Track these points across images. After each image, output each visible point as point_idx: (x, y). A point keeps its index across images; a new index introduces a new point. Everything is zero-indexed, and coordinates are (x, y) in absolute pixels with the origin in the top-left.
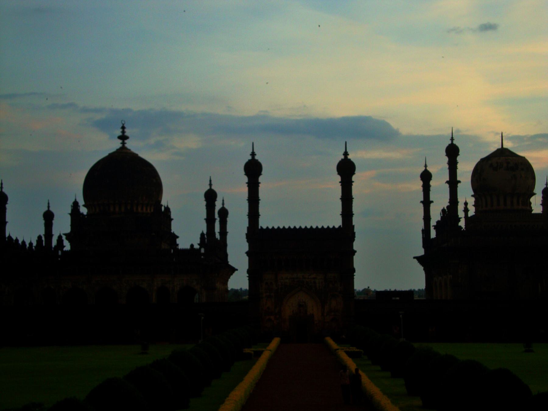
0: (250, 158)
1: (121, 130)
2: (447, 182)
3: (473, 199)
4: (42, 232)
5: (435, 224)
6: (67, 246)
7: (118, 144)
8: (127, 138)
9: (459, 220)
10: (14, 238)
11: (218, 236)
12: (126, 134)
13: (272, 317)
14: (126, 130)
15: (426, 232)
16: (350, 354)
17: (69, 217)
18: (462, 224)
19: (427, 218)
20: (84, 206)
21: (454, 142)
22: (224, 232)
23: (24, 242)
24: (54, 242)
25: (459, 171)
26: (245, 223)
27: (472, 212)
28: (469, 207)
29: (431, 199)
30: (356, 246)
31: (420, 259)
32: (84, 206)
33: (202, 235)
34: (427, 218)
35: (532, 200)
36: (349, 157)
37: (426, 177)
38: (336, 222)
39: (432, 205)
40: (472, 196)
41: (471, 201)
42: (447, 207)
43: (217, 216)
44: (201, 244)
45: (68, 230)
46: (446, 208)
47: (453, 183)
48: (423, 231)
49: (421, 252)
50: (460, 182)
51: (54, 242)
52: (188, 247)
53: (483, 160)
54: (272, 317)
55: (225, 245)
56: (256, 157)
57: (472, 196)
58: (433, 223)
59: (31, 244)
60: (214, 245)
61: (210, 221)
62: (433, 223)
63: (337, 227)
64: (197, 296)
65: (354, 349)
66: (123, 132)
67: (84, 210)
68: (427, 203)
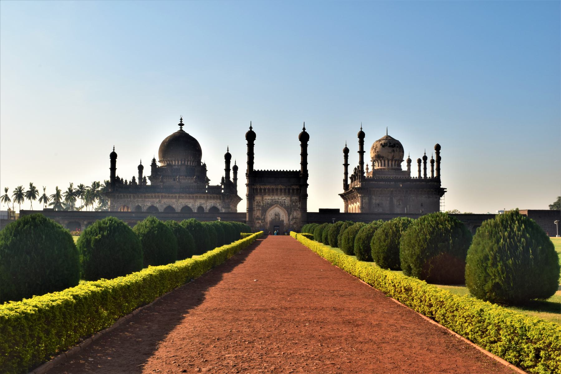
0: (249, 130)
2: (358, 152)
6: (149, 183)
7: (178, 129)
8: (183, 125)
9: (364, 173)
11: (231, 179)
13: (260, 221)
15: (346, 181)
17: (150, 167)
18: (365, 175)
20: (159, 161)
23: (126, 181)
27: (371, 169)
31: (341, 195)
32: (159, 161)
33: (223, 178)
34: (346, 173)
35: (402, 164)
37: (346, 151)
41: (370, 164)
42: (358, 167)
43: (231, 167)
44: (223, 183)
45: (150, 174)
47: (362, 152)
49: (342, 191)
53: (377, 141)
56: (253, 130)
58: (349, 175)
60: (229, 185)
61: (227, 170)
66: (181, 122)
67: (159, 164)
68: (346, 165)
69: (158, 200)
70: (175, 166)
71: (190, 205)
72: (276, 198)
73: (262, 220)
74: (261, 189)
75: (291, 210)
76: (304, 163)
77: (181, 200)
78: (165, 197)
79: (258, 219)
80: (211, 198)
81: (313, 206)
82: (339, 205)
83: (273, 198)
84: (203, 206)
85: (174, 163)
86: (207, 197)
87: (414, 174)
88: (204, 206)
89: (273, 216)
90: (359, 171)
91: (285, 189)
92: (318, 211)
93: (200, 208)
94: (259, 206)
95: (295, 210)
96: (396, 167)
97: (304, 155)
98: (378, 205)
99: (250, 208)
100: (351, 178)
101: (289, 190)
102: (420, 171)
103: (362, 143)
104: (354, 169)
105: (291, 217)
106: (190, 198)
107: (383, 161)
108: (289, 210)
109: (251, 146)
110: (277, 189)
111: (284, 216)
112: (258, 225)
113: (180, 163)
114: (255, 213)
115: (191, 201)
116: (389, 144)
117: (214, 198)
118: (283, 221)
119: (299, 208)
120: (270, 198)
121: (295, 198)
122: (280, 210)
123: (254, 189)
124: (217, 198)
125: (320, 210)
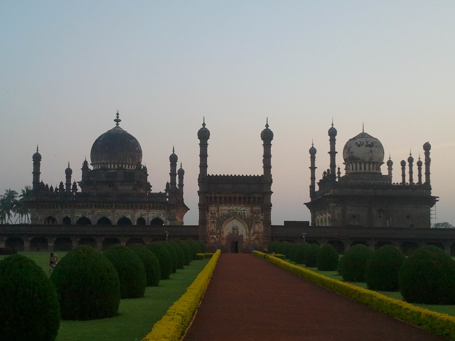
1: (116, 116)
2: (329, 153)
3: (344, 166)
5: (319, 182)
6: (79, 190)
7: (114, 125)
10: (45, 184)
12: (119, 118)
13: (215, 236)
14: (119, 116)
15: (312, 187)
18: (337, 180)
20: (91, 164)
21: (334, 127)
24: (71, 188)
25: (336, 146)
26: (197, 171)
28: (340, 170)
30: (273, 188)
32: (91, 164)
33: (168, 184)
36: (269, 128)
37: (313, 152)
38: (260, 172)
39: (316, 169)
40: (344, 163)
42: (328, 170)
46: (326, 171)
47: (333, 153)
48: (310, 186)
49: (309, 200)
50: (337, 153)
52: (158, 192)
54: (215, 236)
56: (206, 127)
57: (344, 163)
58: (317, 181)
61: (173, 174)
62: (317, 181)
63: (260, 175)
64: (164, 224)
66: (118, 117)
67: (91, 167)
69: (88, 211)
70: (111, 169)
71: (129, 217)
72: (234, 208)
74: (216, 198)
76: (267, 166)
77: (118, 211)
78: (99, 207)
79: (213, 233)
80: (153, 208)
81: (278, 218)
82: (305, 215)
83: (231, 208)
84: (144, 217)
85: (109, 166)
86: (149, 207)
87: (397, 179)
88: (146, 217)
89: (231, 231)
90: (330, 176)
91: (245, 198)
92: (283, 225)
93: (141, 221)
94: (214, 218)
95: (257, 223)
96: (375, 171)
97: (267, 157)
98: (354, 216)
99: (203, 221)
100: (319, 184)
101: (249, 198)
103: (333, 141)
104: (323, 173)
105: (252, 232)
106: (128, 208)
107: (358, 164)
109: (204, 146)
110: (235, 198)
111: (242, 230)
112: (212, 241)
113: (116, 167)
115: (131, 211)
116: (365, 143)
117: (157, 208)
119: (261, 220)
120: (227, 208)
121: (256, 208)
122: (240, 223)
123: (207, 197)
124: (160, 208)
125: (285, 222)
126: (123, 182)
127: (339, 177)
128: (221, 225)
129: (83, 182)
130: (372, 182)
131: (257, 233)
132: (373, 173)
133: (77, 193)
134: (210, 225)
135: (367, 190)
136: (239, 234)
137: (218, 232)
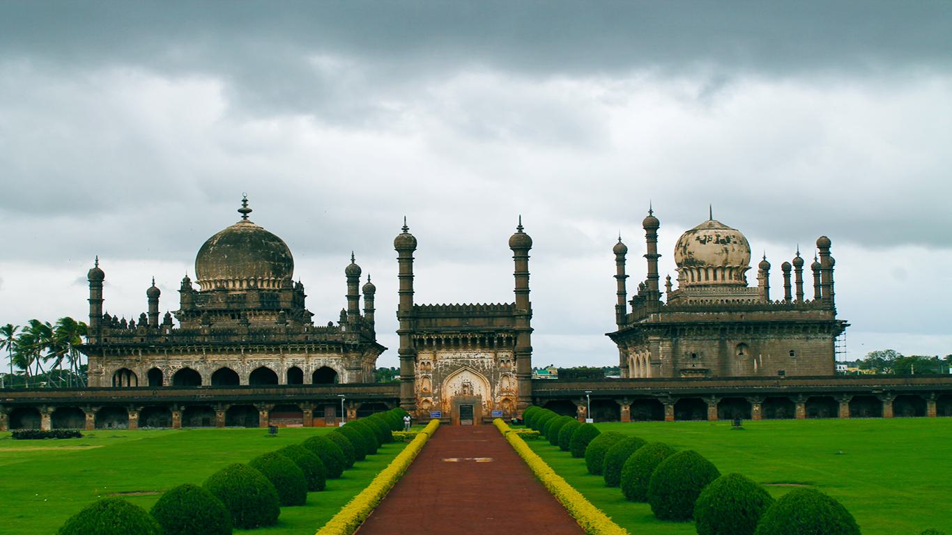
4: (145, 308)
5: (632, 299)
6: (177, 325)
9: (660, 295)
10: (112, 317)
11: (362, 313)
16: (525, 437)
18: (664, 299)
19: (622, 293)
22: (370, 310)
24: (161, 321)
28: (671, 281)
29: (626, 274)
33: (343, 313)
51: (161, 321)
54: (430, 399)
55: (373, 323)
58: (629, 298)
59: (132, 322)
62: (629, 298)
65: (529, 431)
73: (435, 395)
75: (496, 377)
79: (426, 393)
89: (459, 389)
95: (505, 375)
100: (631, 302)
102: (788, 287)
108: (492, 377)
111: (481, 388)
114: (418, 382)
118: (480, 397)
119: (514, 372)
122: (474, 376)
126: (259, 310)
127: (669, 291)
128: (441, 382)
129: (183, 312)
130: (730, 299)
131: (506, 392)
132: (729, 285)
133: (174, 332)
134: (420, 381)
135: (716, 314)
136: (475, 394)
137: (436, 391)
